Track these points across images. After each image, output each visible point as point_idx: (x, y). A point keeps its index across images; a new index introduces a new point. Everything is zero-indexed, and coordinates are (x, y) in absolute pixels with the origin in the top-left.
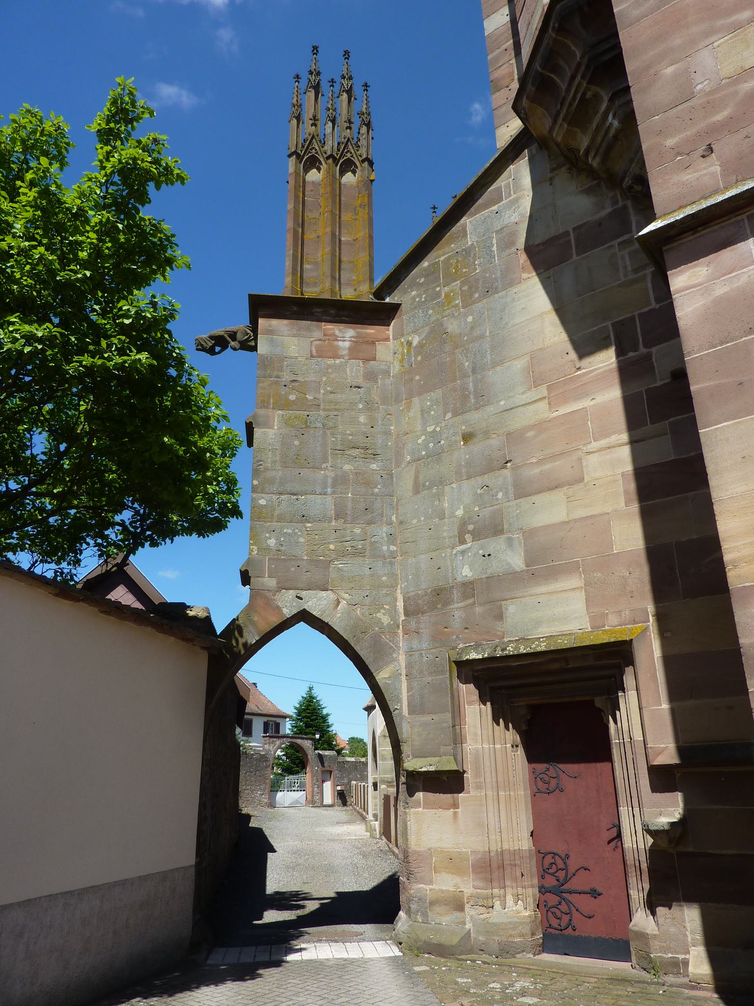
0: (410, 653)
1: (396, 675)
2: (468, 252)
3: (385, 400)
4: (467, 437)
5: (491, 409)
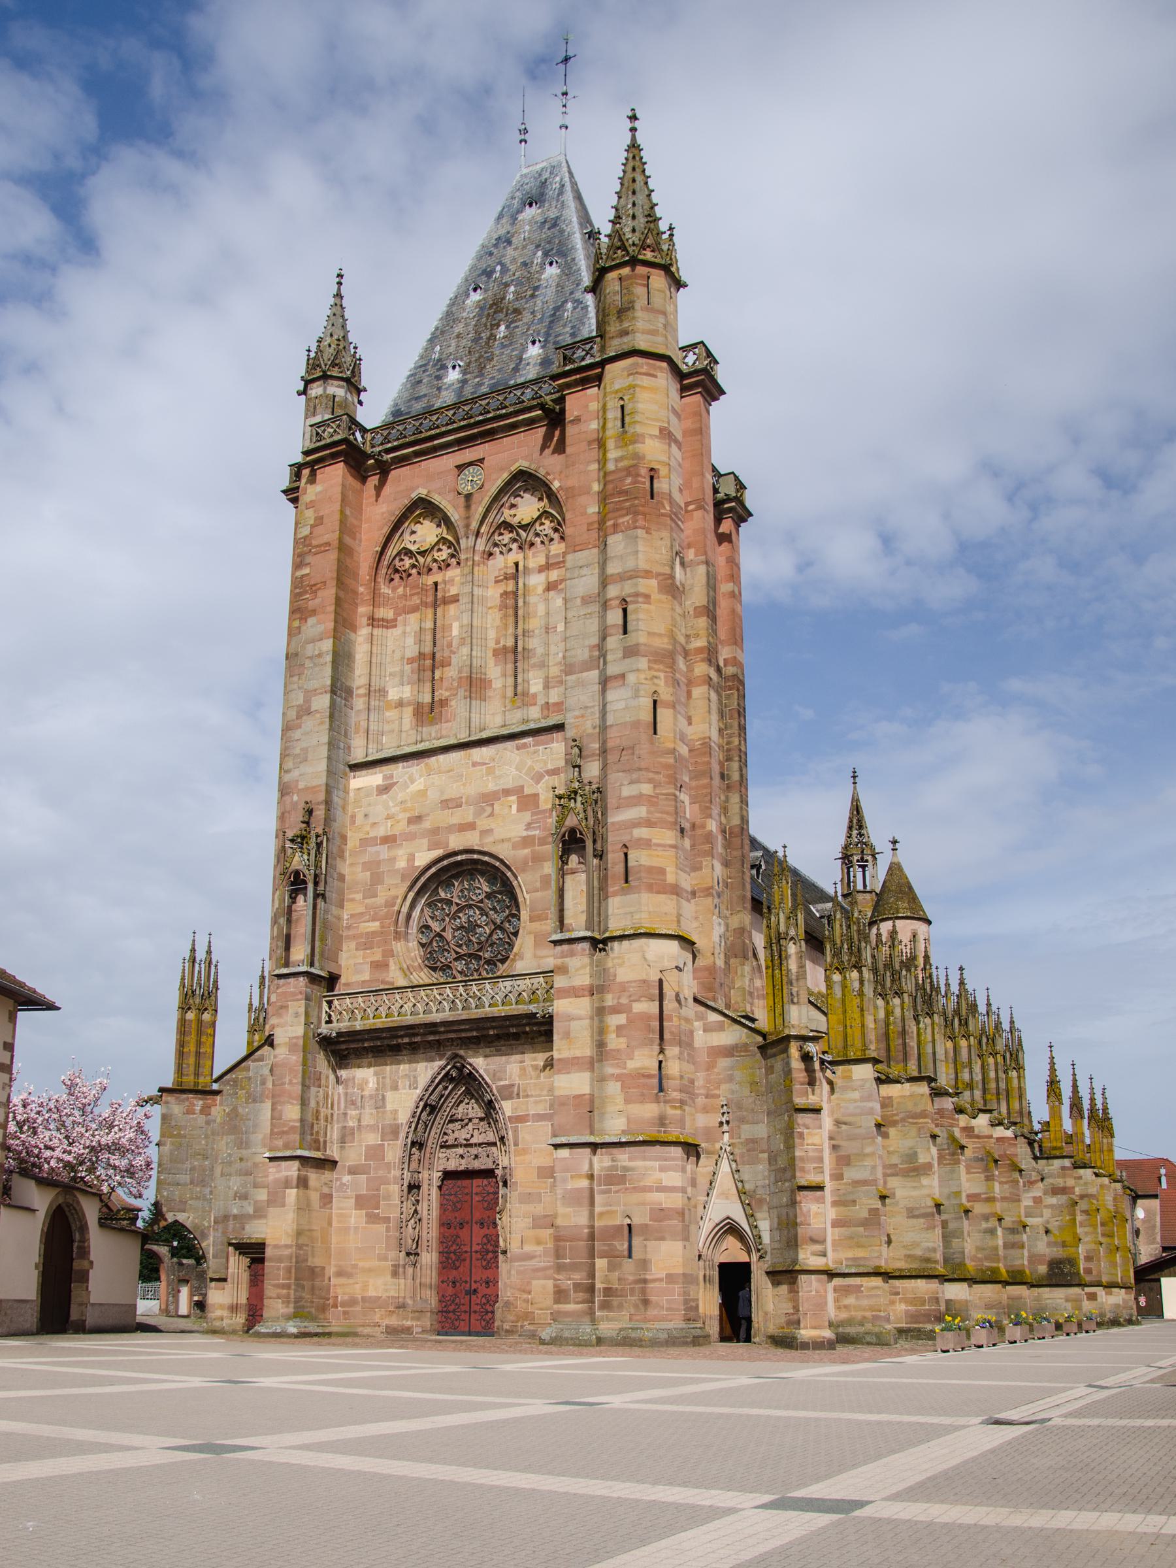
0: (214, 1237)
1: (209, 1245)
2: (250, 1078)
3: (213, 1134)
4: (241, 1159)
5: (250, 1151)
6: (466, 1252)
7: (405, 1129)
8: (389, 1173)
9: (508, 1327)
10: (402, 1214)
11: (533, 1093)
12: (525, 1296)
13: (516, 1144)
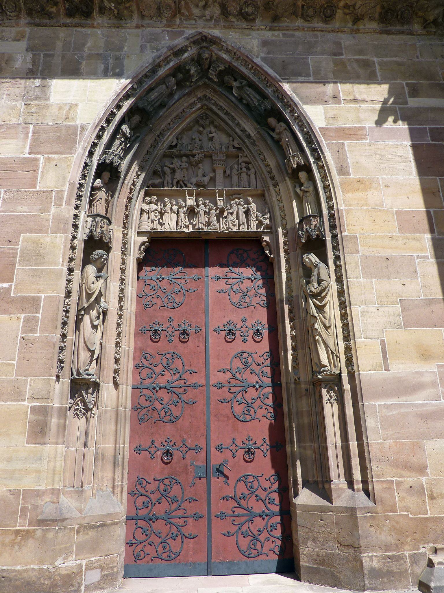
6: (195, 386)
7: (90, 136)
8: (45, 209)
9: (376, 564)
10: (68, 294)
11: (365, 97)
12: (411, 479)
13: (343, 171)
